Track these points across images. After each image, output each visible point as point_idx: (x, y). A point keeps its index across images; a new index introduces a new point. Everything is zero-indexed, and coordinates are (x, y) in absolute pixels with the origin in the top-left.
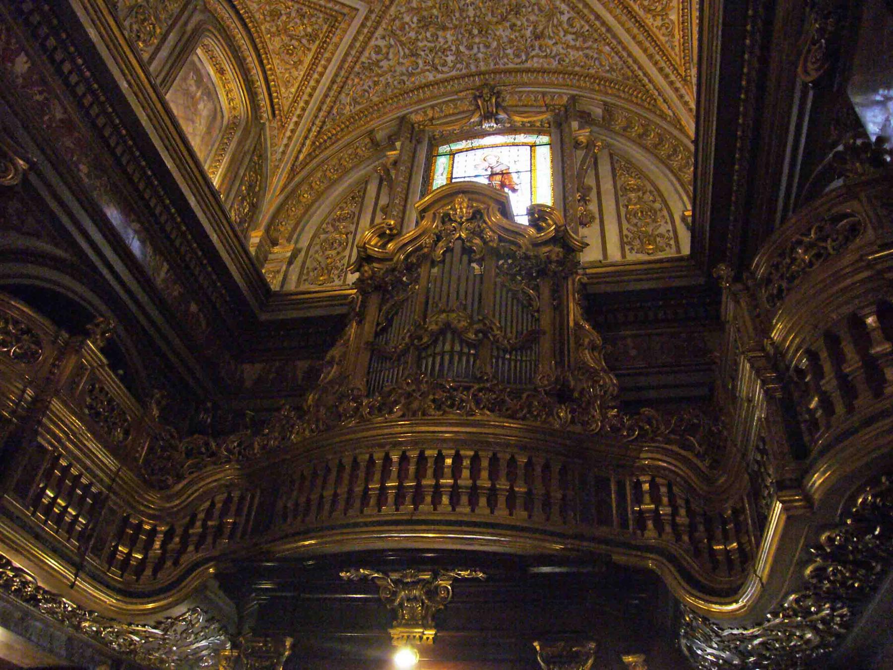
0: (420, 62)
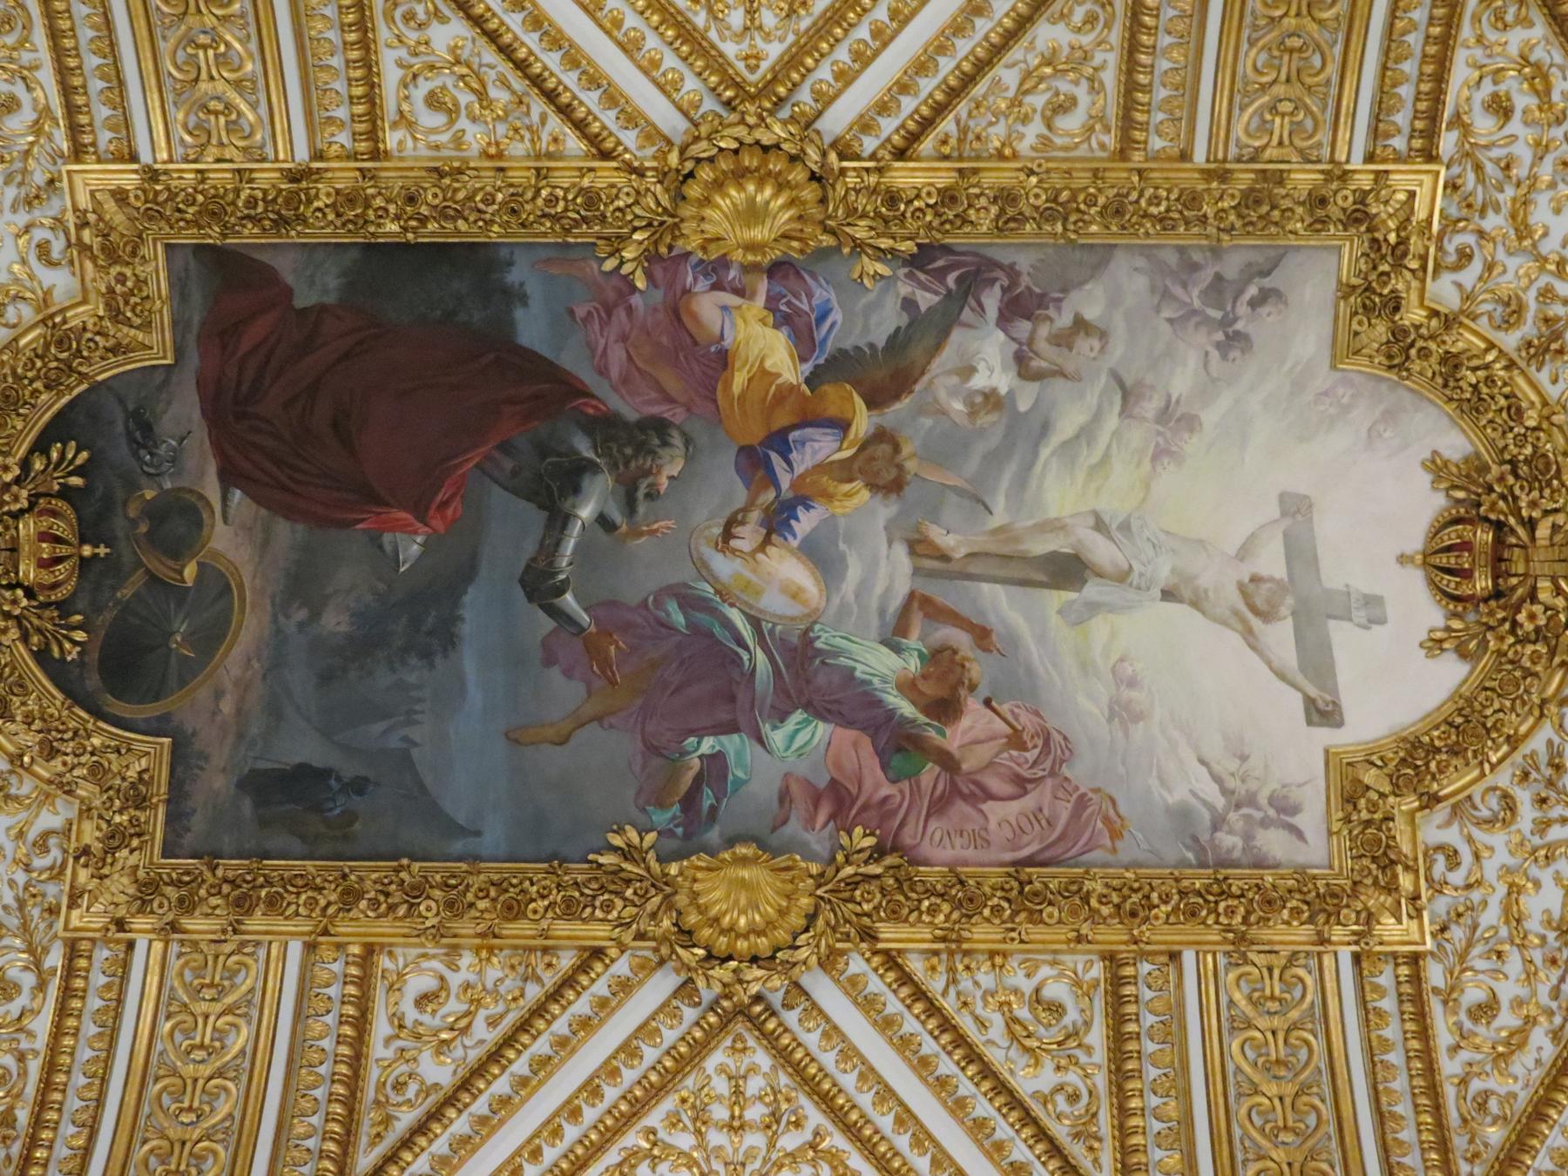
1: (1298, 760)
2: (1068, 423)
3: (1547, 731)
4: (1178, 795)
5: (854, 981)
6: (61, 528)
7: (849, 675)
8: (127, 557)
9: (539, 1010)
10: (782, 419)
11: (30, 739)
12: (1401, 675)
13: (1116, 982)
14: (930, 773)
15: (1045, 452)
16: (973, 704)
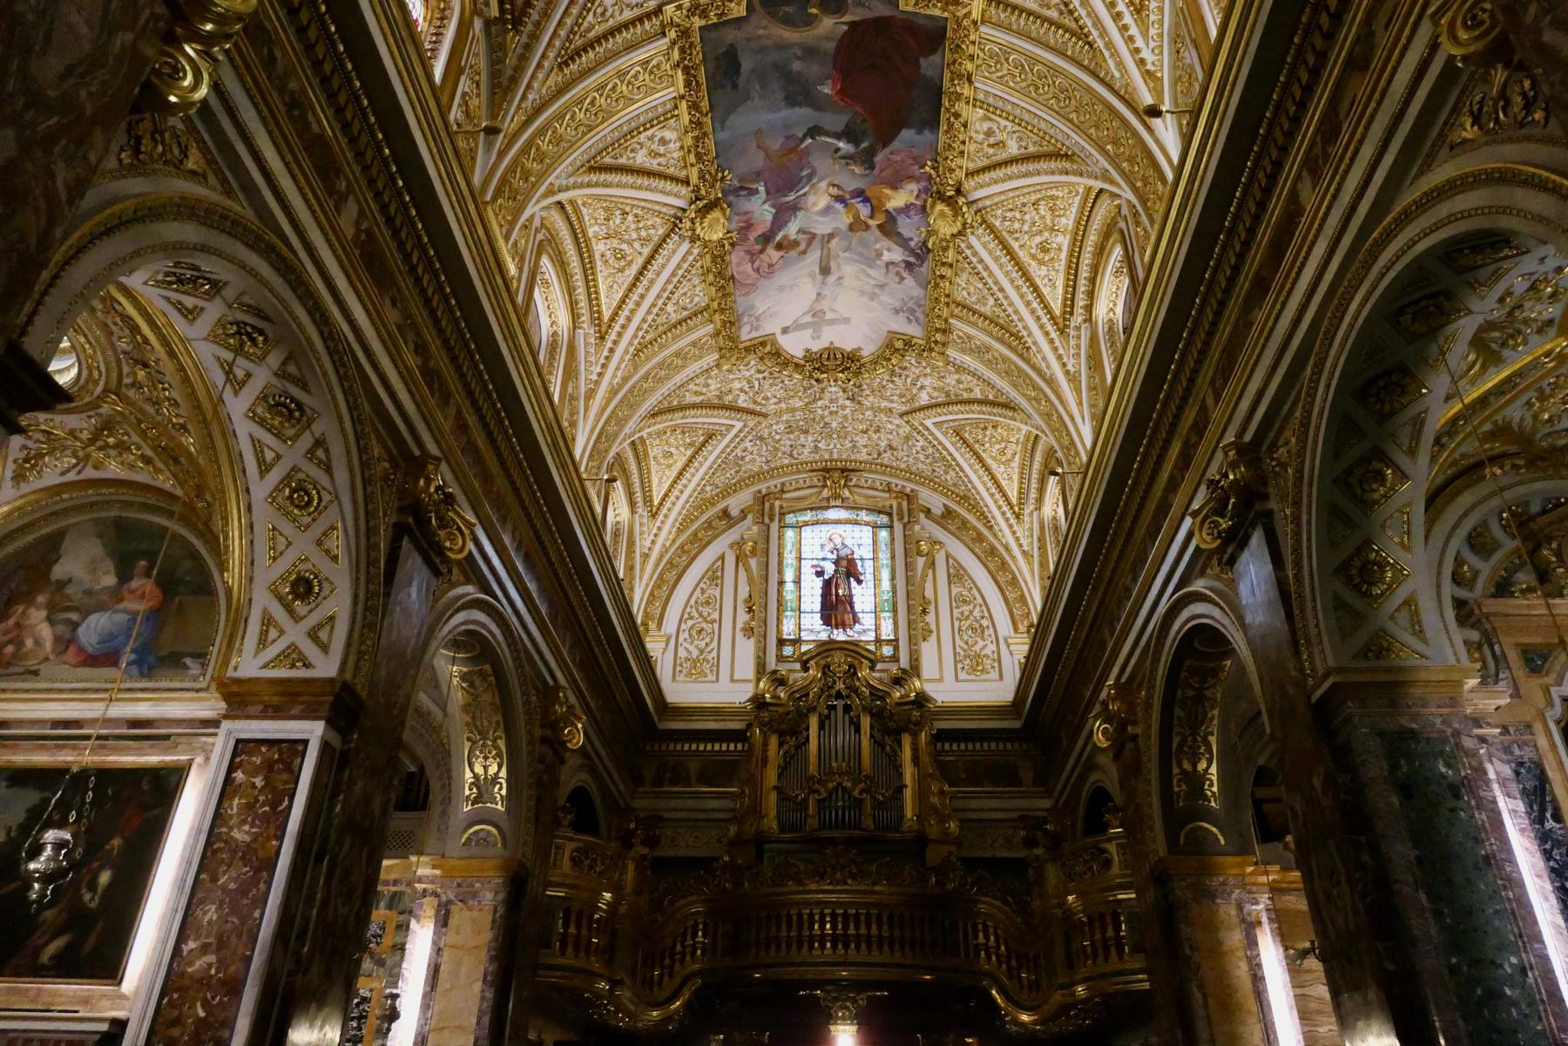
1: (771, 327)
2: (870, 271)
14: (759, 247)
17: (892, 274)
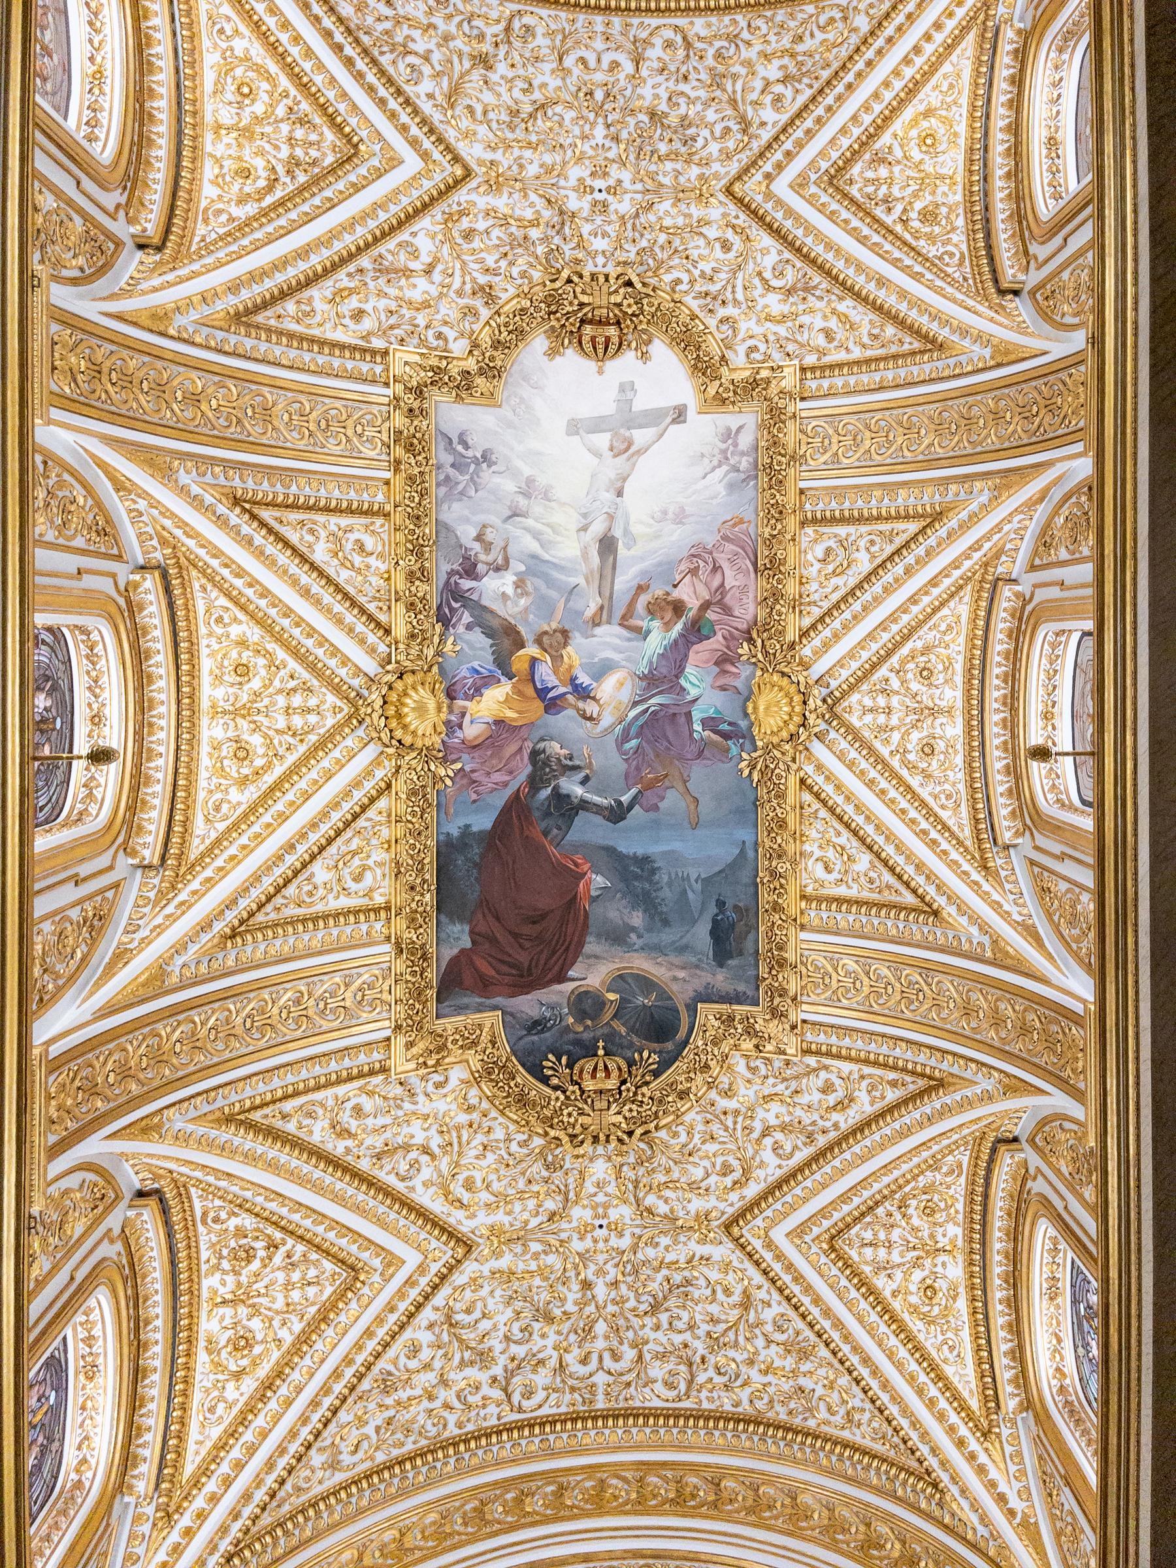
0: (710, 61)
1: (704, 428)
2: (534, 546)
3: (688, 300)
4: (721, 489)
5: (815, 653)
6: (589, 1067)
7: (662, 656)
8: (606, 1030)
9: (832, 810)
10: (530, 692)
11: (699, 1079)
12: (658, 374)
13: (814, 521)
14: (711, 615)
15: (547, 557)
16: (676, 594)
17: (498, 544)
